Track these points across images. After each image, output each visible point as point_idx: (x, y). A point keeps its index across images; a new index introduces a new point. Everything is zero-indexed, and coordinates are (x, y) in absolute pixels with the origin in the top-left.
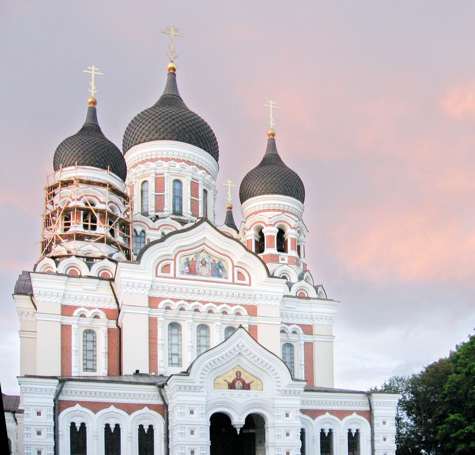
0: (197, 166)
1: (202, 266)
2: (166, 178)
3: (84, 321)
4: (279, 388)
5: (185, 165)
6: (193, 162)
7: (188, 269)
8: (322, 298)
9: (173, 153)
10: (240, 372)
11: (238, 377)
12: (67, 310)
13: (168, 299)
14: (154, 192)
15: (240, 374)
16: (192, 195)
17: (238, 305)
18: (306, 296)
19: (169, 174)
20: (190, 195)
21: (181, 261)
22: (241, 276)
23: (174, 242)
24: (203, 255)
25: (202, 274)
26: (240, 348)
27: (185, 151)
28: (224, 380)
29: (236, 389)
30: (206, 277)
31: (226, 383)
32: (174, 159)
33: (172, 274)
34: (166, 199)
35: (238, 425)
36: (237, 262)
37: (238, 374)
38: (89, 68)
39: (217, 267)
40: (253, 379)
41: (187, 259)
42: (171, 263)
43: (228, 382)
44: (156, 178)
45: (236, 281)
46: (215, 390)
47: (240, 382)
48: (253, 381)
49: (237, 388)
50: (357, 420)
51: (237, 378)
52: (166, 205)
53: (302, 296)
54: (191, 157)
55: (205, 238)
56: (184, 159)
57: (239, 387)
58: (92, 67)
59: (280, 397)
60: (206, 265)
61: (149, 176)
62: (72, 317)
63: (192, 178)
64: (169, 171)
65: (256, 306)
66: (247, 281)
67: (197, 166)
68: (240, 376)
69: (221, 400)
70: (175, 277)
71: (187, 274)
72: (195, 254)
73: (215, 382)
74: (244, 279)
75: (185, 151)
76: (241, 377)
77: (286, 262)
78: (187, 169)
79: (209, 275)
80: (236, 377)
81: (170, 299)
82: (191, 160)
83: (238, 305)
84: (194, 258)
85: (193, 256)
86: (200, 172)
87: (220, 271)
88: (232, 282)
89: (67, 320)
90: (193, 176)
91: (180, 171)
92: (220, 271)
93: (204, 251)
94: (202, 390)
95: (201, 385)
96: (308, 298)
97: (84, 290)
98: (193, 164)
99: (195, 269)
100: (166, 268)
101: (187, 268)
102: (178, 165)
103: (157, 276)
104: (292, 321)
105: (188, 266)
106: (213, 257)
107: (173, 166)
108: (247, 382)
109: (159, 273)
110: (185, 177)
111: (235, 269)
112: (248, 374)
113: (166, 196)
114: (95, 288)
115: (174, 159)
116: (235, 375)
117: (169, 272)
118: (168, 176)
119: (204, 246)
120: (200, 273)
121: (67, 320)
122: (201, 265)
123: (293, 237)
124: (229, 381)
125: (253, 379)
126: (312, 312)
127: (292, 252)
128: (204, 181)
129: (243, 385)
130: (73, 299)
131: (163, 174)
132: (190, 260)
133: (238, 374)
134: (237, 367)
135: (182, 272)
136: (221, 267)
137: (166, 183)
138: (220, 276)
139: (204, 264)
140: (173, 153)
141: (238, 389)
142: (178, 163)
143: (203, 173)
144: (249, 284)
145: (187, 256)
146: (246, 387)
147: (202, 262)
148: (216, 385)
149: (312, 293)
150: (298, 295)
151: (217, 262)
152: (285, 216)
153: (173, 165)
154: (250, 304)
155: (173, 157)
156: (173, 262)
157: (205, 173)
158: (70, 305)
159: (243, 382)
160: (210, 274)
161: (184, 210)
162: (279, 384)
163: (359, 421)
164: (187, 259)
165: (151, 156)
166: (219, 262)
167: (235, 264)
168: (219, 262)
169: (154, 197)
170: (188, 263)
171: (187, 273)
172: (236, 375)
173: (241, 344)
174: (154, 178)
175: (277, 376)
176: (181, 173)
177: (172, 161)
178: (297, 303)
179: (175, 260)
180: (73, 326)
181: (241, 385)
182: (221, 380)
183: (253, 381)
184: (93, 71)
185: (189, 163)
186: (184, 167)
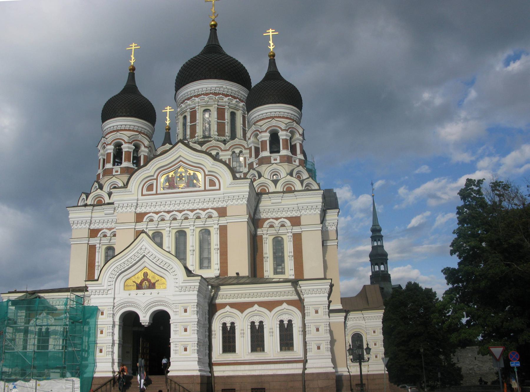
0: (223, 94)
1: (179, 180)
2: (197, 110)
3: (105, 241)
4: (177, 285)
5: (212, 97)
6: (220, 92)
7: (168, 184)
8: (313, 188)
9: (220, 89)
10: (147, 273)
11: (145, 278)
12: (94, 233)
13: (151, 213)
14: (189, 124)
15: (147, 275)
16: (218, 120)
17: (210, 209)
18: (293, 189)
19: (199, 107)
20: (216, 120)
21: (162, 179)
22: (212, 183)
23: (154, 166)
24: (181, 170)
25: (179, 186)
26: (144, 251)
27: (211, 86)
28: (133, 282)
29: (143, 289)
30: (182, 188)
31: (135, 284)
32: (203, 94)
33: (154, 192)
34: (197, 127)
35: (143, 323)
36: (207, 172)
37: (146, 274)
38: (267, 31)
39: (193, 177)
40: (157, 278)
41: (168, 176)
42: (154, 182)
43: (136, 283)
44: (191, 112)
45: (208, 187)
46: (125, 291)
47: (147, 282)
48: (158, 280)
49: (143, 288)
50: (230, 313)
51: (144, 278)
52: (197, 132)
53: (289, 190)
54: (216, 89)
55: (180, 156)
56: (211, 92)
57: (146, 287)
58: (269, 30)
59: (178, 293)
60: (183, 179)
61: (186, 111)
62: (96, 238)
63: (218, 105)
64: (199, 104)
65: (226, 208)
66: (217, 187)
67: (223, 94)
68: (147, 277)
69: (126, 300)
70: (157, 194)
71: (167, 189)
72: (174, 171)
73: (126, 285)
74: (215, 185)
75: (211, 86)
76: (148, 276)
77: (278, 161)
78: (206, 99)
79: (186, 187)
80: (143, 277)
81: (153, 213)
82: (217, 91)
83: (210, 209)
84: (173, 174)
85: (172, 173)
86: (226, 99)
87: (195, 181)
88: (204, 189)
89: (93, 241)
90: (219, 103)
91: (208, 102)
92: (195, 181)
93: (181, 167)
94: (110, 292)
95: (109, 288)
96: (295, 191)
97: (105, 214)
98: (219, 94)
99: (174, 184)
100: (150, 188)
101: (167, 184)
102: (206, 98)
103: (142, 195)
104: (279, 215)
105: (168, 183)
106: (188, 170)
107: (203, 100)
108: (153, 281)
109: (145, 192)
110: (212, 106)
111: (207, 177)
112: (153, 274)
113: (197, 125)
114: (113, 211)
115: (203, 94)
116: (143, 276)
117: (153, 191)
118: (198, 109)
119: (181, 163)
120: (178, 186)
121: (93, 241)
122: (179, 179)
123: (284, 137)
124: (137, 282)
125: (157, 278)
126: (297, 204)
127: (284, 152)
128: (229, 105)
129: (150, 285)
130: (98, 223)
131: (194, 108)
132: (170, 176)
133: (146, 274)
134: (145, 269)
135: (164, 188)
136: (197, 180)
137: (197, 114)
138: (194, 186)
139: (181, 177)
140: (220, 89)
141: (145, 289)
142: (207, 96)
143: (228, 99)
144: (218, 188)
145: (167, 174)
146: (152, 286)
147: (179, 177)
148: (126, 287)
149: (298, 186)
150: (285, 190)
151: (192, 174)
152: (275, 121)
153: (203, 99)
154: (220, 207)
155: (203, 93)
156: (155, 181)
157: (231, 99)
158: (96, 228)
159: (149, 281)
160: (186, 186)
161: (212, 133)
162: (177, 281)
163: (231, 313)
164: (168, 176)
165: (223, 91)
166: (194, 174)
167: (207, 173)
168: (194, 174)
169: (189, 127)
170: (168, 180)
171: (167, 188)
172: (144, 276)
173: (143, 247)
174: (188, 112)
175: (175, 273)
176: (208, 103)
177: (203, 96)
178: (282, 197)
179: (157, 179)
180: (98, 246)
181: (148, 285)
182: (130, 282)
183: (158, 280)
184: (271, 32)
185: (215, 94)
186: (212, 98)
